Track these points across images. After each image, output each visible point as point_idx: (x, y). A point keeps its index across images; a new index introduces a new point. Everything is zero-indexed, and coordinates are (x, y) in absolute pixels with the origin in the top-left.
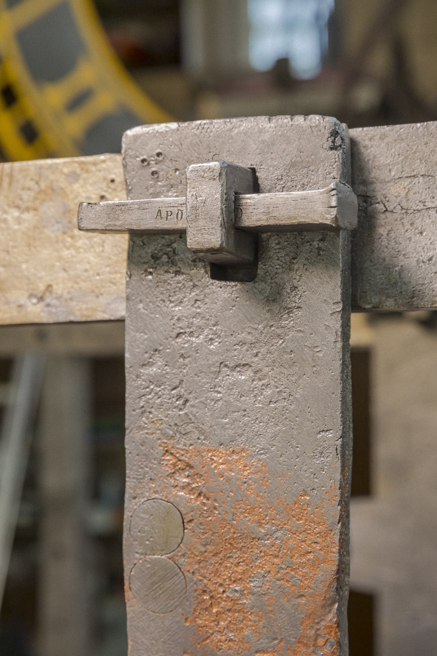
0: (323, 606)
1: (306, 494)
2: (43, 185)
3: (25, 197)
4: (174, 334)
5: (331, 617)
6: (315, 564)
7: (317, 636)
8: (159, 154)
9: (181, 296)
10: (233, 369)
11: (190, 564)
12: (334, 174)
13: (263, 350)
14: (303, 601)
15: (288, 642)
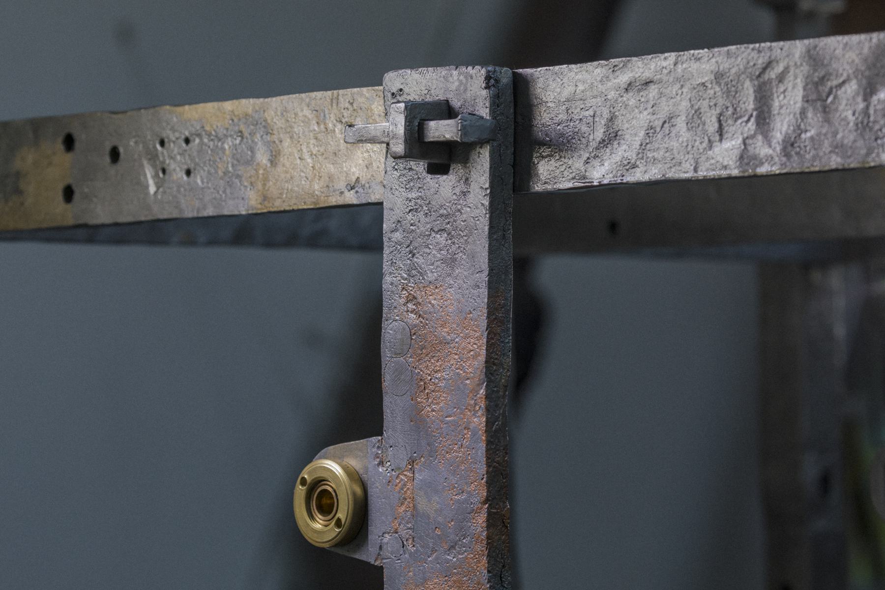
0: (478, 385)
1: (471, 313)
2: (355, 105)
3: (345, 114)
4: (407, 210)
5: (482, 391)
6: (475, 357)
7: (476, 404)
8: (401, 90)
9: (412, 184)
10: (437, 233)
11: (413, 362)
12: (488, 105)
13: (452, 220)
14: (468, 382)
15: (461, 409)
